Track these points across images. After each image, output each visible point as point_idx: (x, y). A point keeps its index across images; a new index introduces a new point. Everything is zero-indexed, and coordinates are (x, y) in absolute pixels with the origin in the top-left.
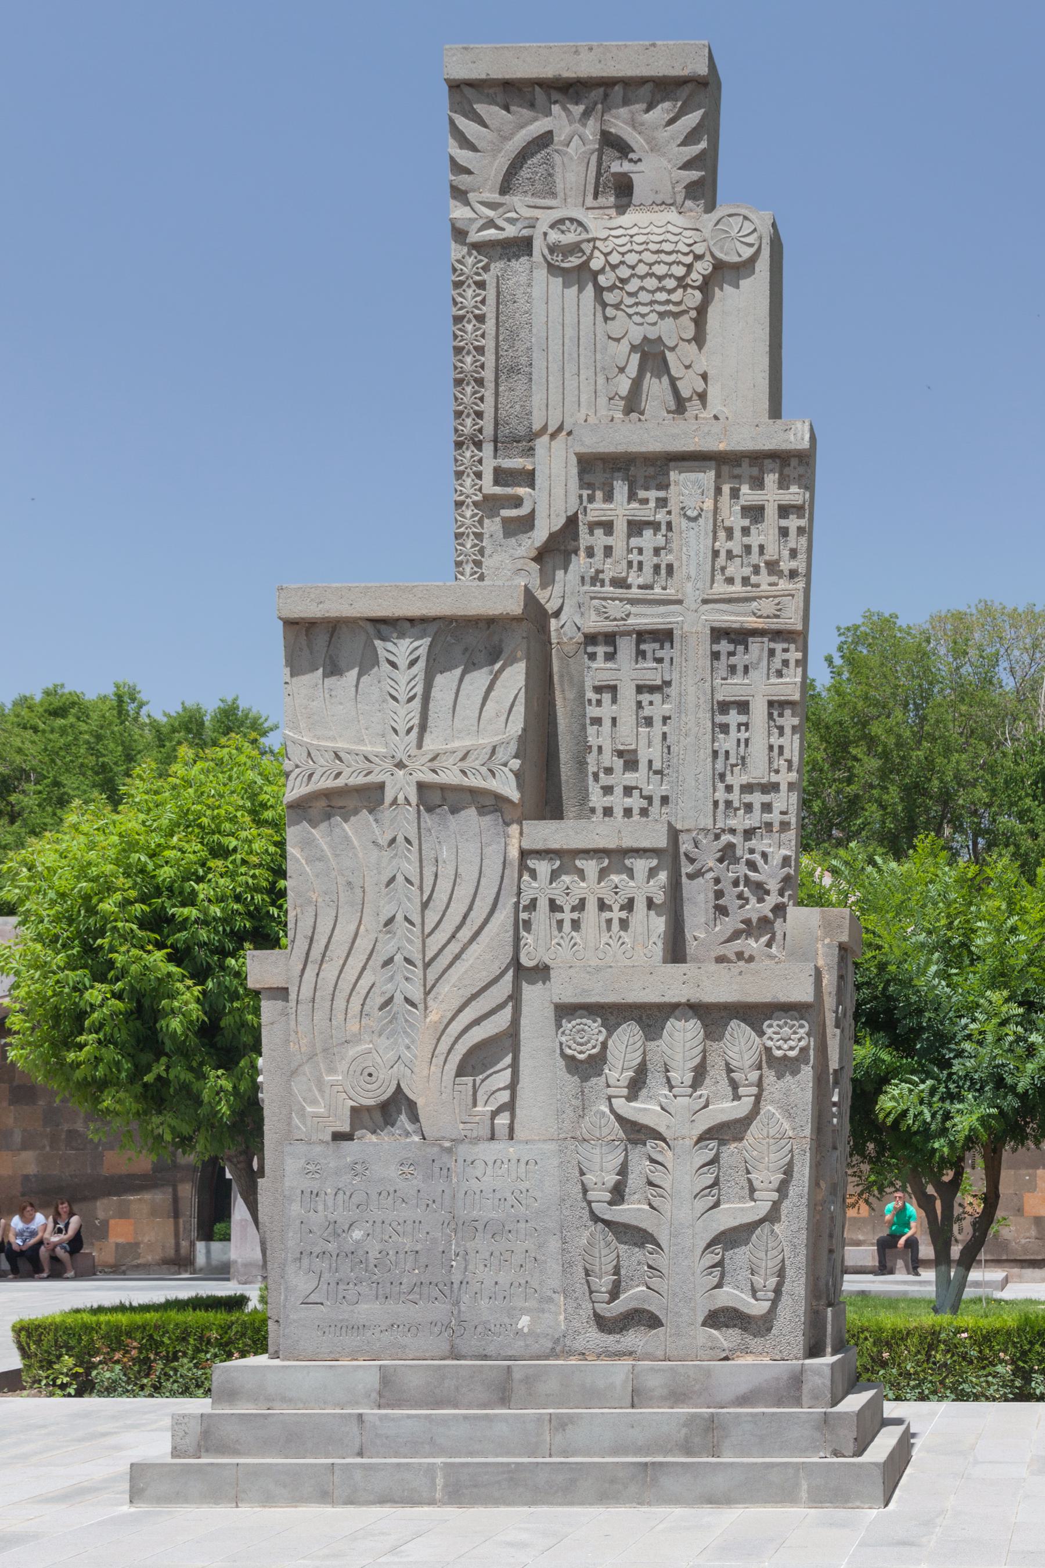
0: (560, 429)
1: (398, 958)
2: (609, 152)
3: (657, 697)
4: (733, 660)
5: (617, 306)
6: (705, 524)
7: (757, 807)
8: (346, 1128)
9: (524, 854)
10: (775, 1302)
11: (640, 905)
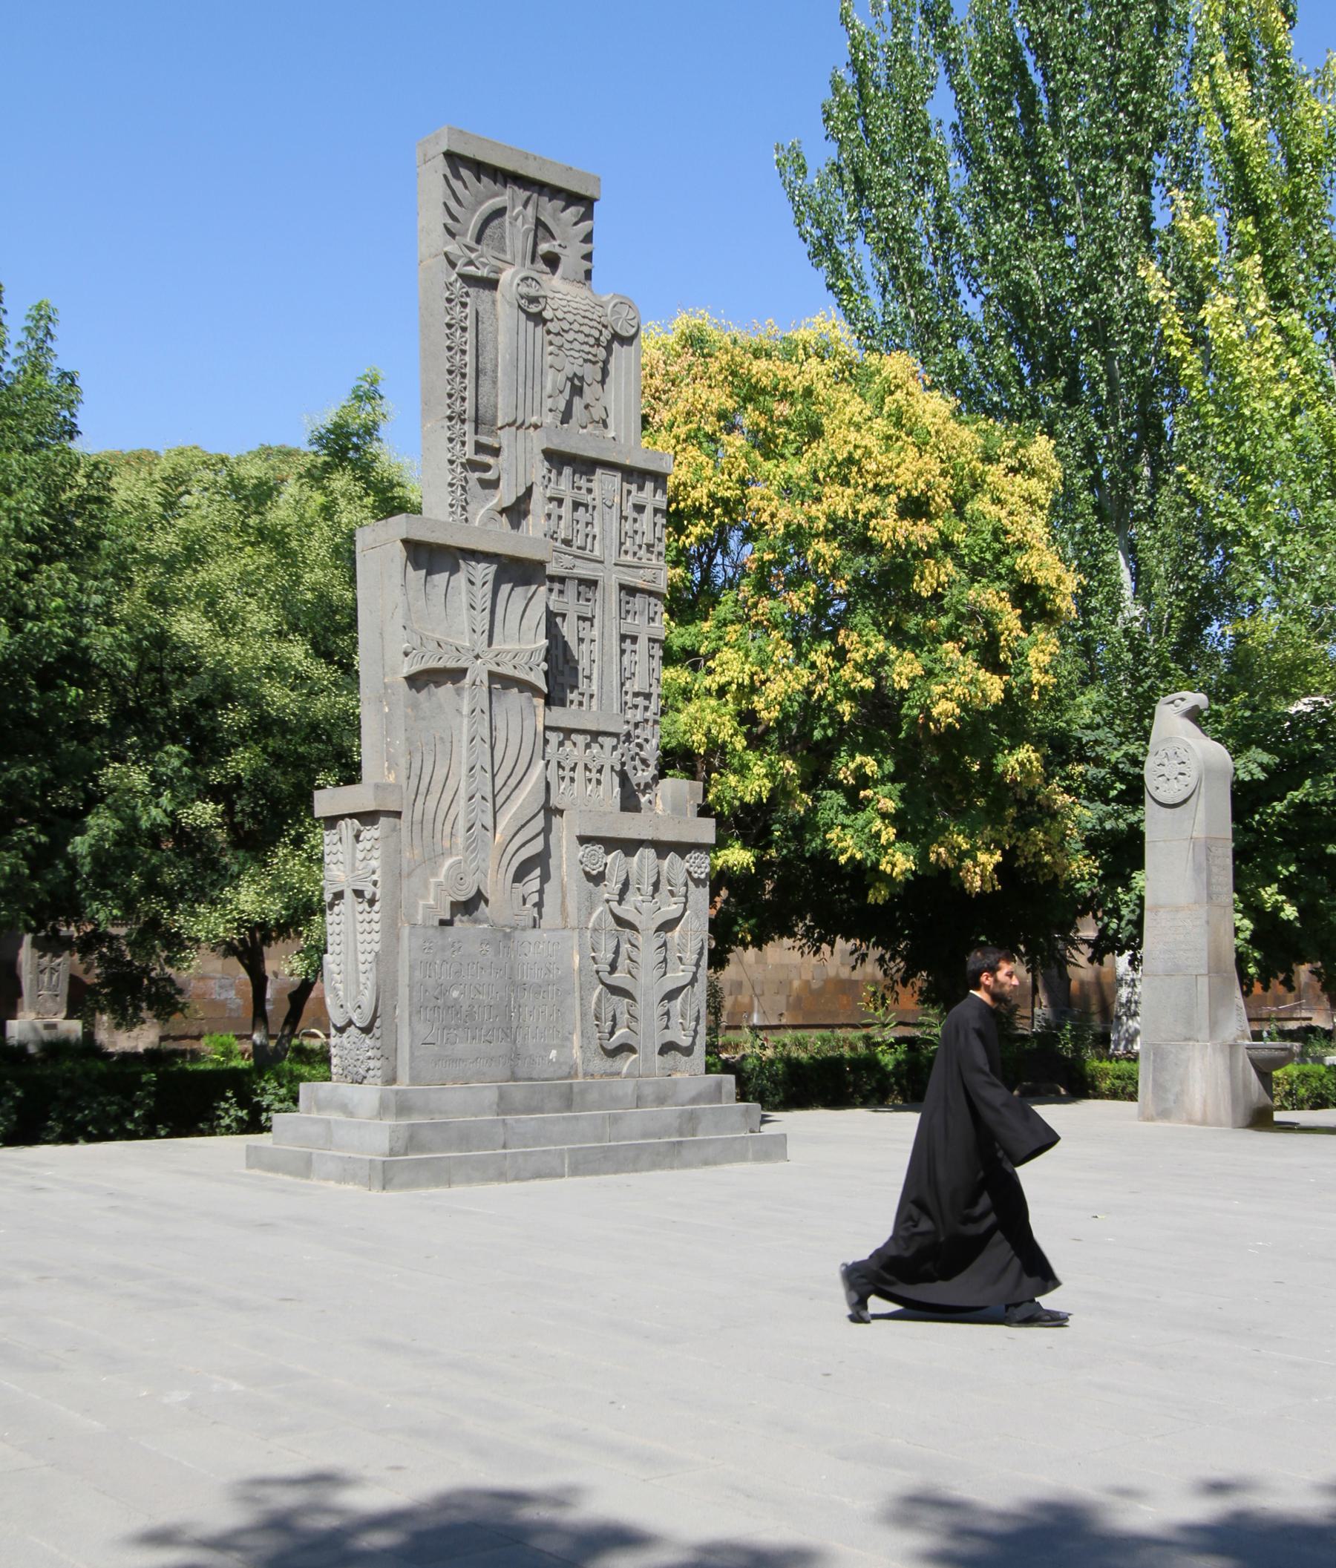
0: (523, 423)
1: (478, 796)
2: (541, 232)
3: (588, 623)
4: (628, 607)
5: (560, 347)
6: (615, 510)
7: (641, 708)
8: (448, 917)
9: (546, 728)
10: (694, 1037)
11: (607, 770)
